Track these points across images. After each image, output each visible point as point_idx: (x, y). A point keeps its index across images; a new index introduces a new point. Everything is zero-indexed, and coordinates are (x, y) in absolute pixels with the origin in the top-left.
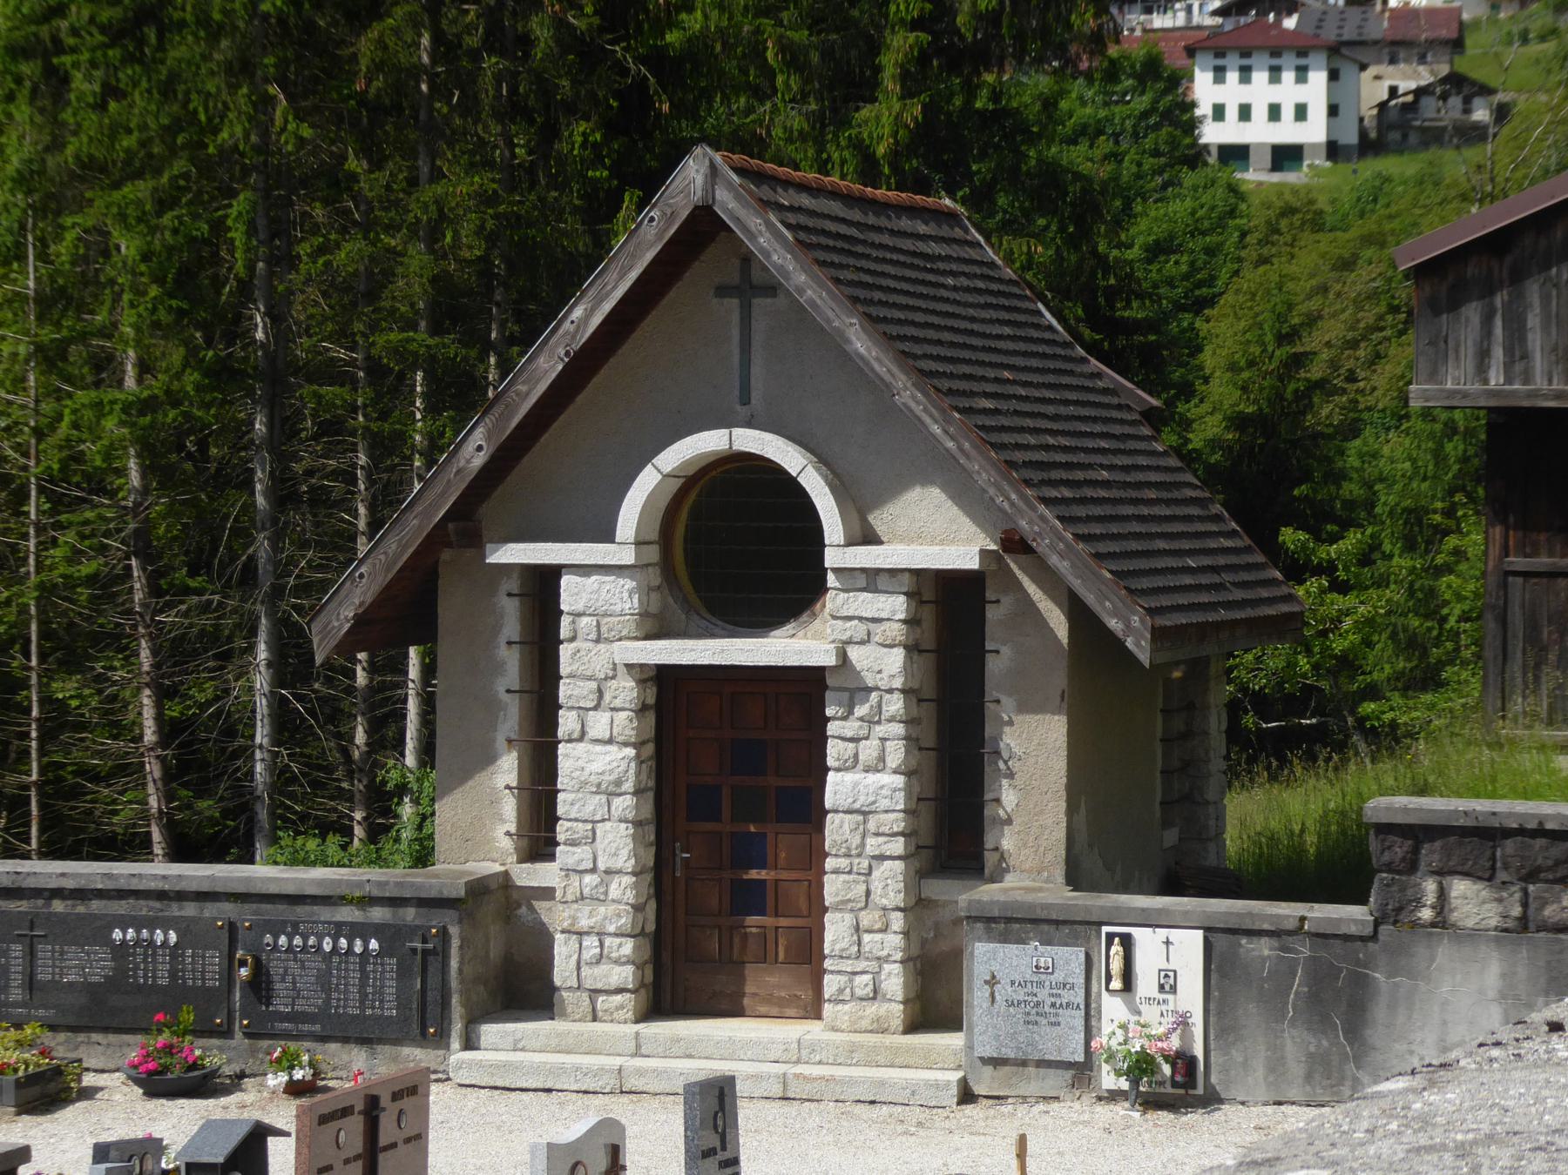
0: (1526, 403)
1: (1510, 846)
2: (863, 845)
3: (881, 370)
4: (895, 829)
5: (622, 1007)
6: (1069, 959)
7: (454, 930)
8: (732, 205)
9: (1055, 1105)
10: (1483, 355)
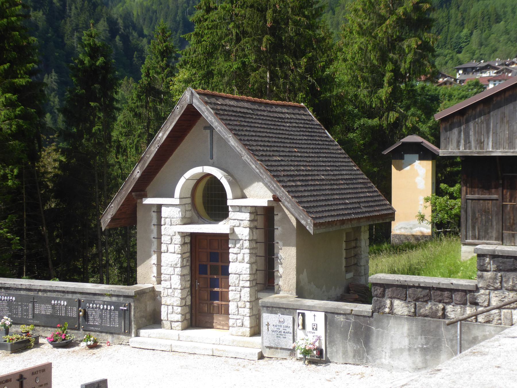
0: (470, 155)
1: (410, 291)
2: (239, 283)
3: (238, 150)
4: (247, 279)
5: (178, 326)
6: (288, 319)
7: (132, 304)
8: (198, 103)
9: (285, 361)
10: (459, 142)
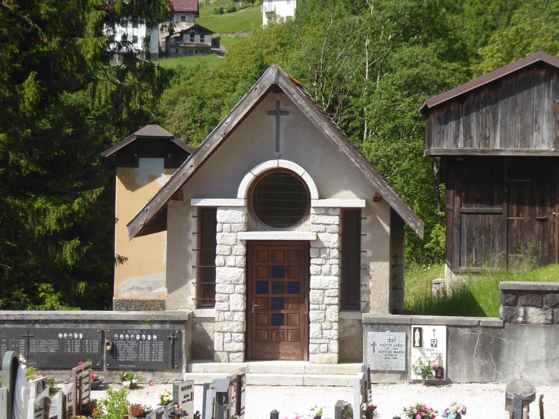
0: (471, 154)
1: (548, 296)
2: (323, 300)
3: (335, 140)
4: (335, 295)
5: (239, 357)
6: (400, 337)
7: (183, 331)
8: (285, 84)
9: (395, 385)
10: (456, 137)
